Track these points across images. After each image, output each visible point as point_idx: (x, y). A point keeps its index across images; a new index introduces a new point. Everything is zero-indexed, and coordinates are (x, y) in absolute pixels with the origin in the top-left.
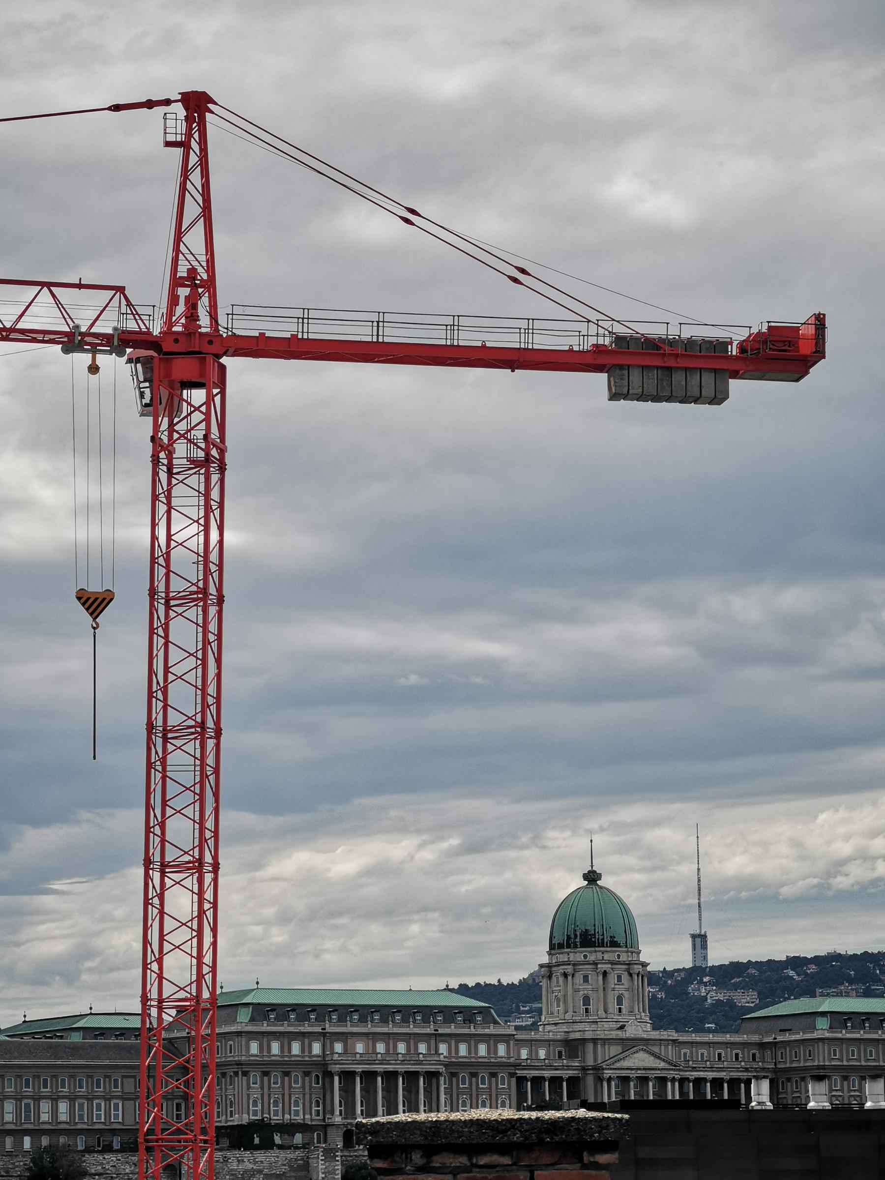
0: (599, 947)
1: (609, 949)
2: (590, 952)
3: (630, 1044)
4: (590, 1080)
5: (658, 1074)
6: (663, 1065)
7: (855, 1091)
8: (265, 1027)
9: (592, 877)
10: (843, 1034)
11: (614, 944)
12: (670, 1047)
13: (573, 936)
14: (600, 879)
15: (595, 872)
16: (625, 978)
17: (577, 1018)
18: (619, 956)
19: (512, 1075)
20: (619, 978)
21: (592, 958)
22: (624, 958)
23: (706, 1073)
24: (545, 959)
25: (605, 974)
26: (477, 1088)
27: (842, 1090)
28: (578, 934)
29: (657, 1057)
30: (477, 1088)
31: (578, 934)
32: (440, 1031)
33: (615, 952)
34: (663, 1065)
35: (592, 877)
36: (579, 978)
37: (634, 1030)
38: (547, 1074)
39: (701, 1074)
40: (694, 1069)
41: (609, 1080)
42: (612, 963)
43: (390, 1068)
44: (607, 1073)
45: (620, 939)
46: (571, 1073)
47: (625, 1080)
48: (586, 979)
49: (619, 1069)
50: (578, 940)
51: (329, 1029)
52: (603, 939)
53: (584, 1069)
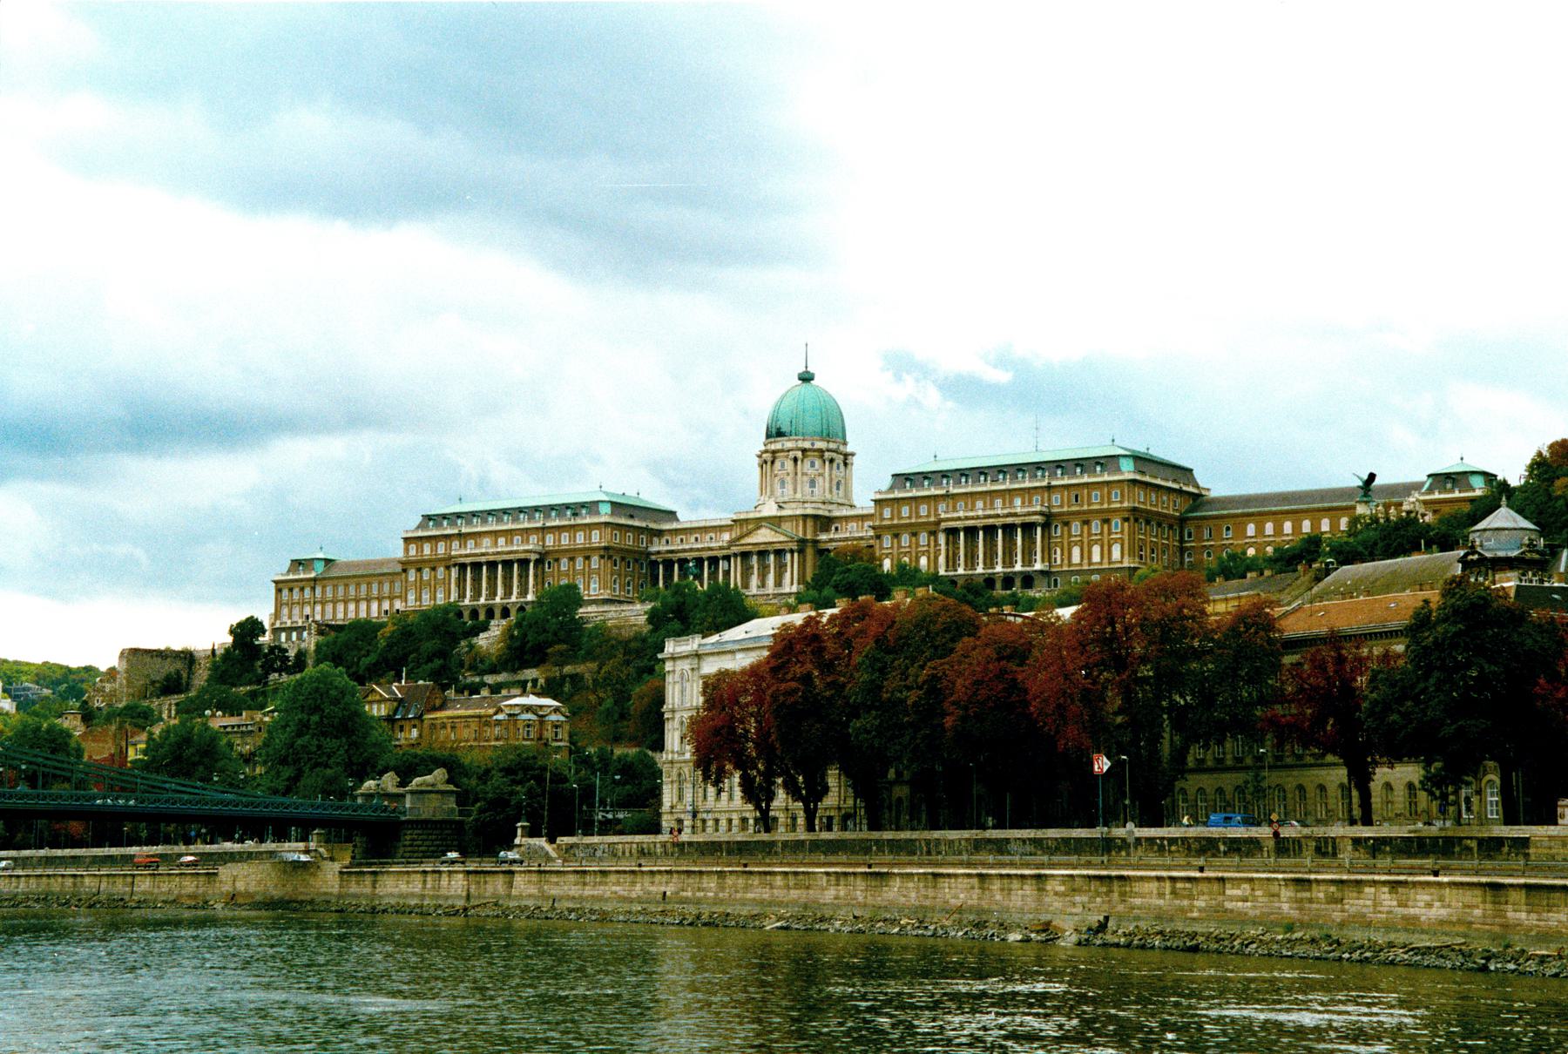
3: (759, 522)
5: (778, 547)
8: (420, 533)
9: (806, 378)
10: (897, 494)
11: (780, 434)
19: (602, 557)
22: (789, 445)
32: (548, 524)
34: (782, 538)
35: (806, 378)
37: (770, 510)
38: (705, 554)
41: (735, 555)
42: (774, 452)
43: (491, 558)
51: (464, 530)
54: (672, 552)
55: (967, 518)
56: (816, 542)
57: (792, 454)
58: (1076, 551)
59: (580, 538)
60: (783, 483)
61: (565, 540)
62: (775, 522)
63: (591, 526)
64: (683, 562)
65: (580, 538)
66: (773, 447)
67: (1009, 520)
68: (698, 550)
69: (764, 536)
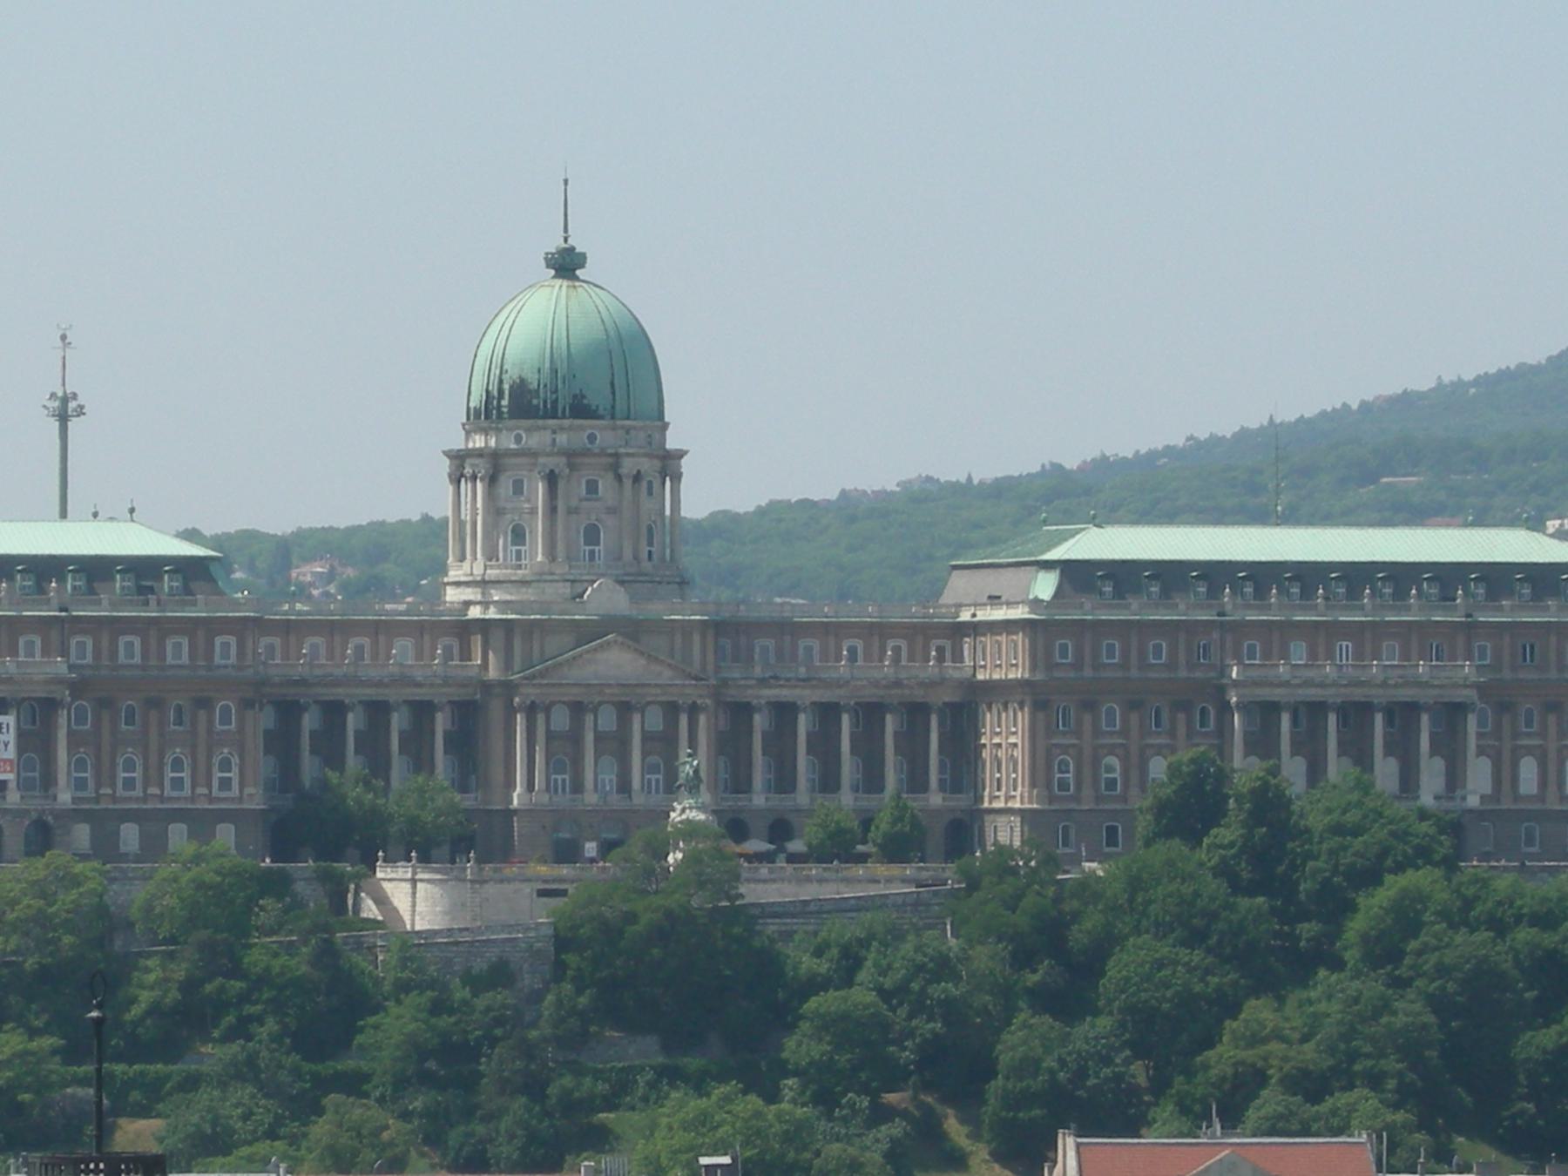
0: (545, 417)
1: (566, 422)
2: (528, 430)
4: (496, 710)
6: (668, 673)
7: (1111, 734)
9: (566, 264)
11: (580, 410)
12: (696, 638)
13: (496, 393)
14: (582, 266)
15: (573, 249)
16: (605, 485)
17: (492, 573)
18: (592, 438)
19: (246, 704)
20: (592, 487)
21: (534, 441)
23: (797, 692)
24: (458, 442)
25: (552, 479)
26: (210, 731)
27: (1124, 732)
28: (506, 387)
29: (652, 659)
30: (210, 731)
31: (506, 387)
33: (582, 428)
36: (505, 486)
39: (785, 694)
40: (763, 682)
42: (571, 455)
44: (531, 693)
45: (597, 397)
46: (458, 694)
47: (577, 709)
48: (518, 487)
49: (553, 685)
50: (505, 402)
52: (555, 402)
53: (486, 686)
54: (303, 682)
55: (1308, 683)
56: (725, 683)
57: (628, 467)
58: (1528, 770)
59: (178, 651)
60: (592, 535)
61: (130, 650)
62: (632, 631)
63: (213, 627)
64: (334, 711)
65: (178, 651)
66: (562, 439)
67: (1406, 694)
68: (379, 684)
69: (616, 663)
